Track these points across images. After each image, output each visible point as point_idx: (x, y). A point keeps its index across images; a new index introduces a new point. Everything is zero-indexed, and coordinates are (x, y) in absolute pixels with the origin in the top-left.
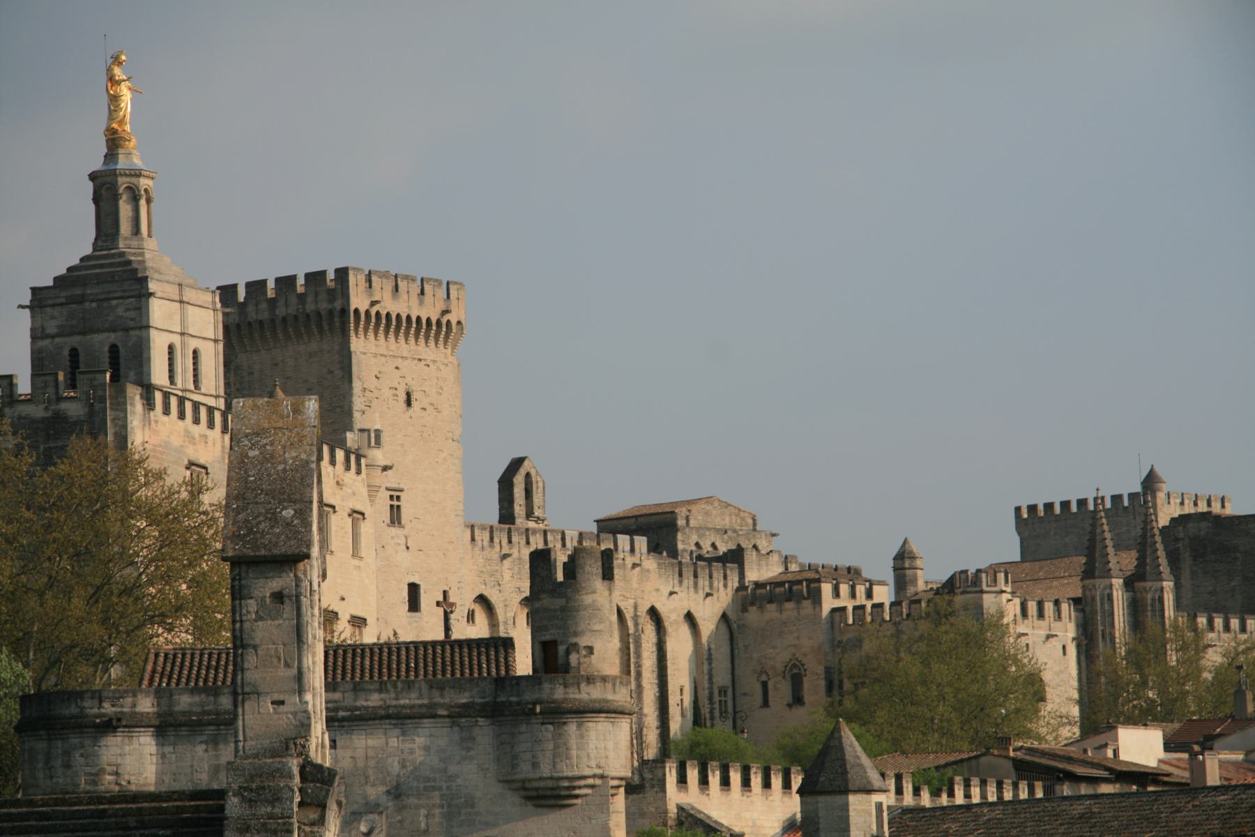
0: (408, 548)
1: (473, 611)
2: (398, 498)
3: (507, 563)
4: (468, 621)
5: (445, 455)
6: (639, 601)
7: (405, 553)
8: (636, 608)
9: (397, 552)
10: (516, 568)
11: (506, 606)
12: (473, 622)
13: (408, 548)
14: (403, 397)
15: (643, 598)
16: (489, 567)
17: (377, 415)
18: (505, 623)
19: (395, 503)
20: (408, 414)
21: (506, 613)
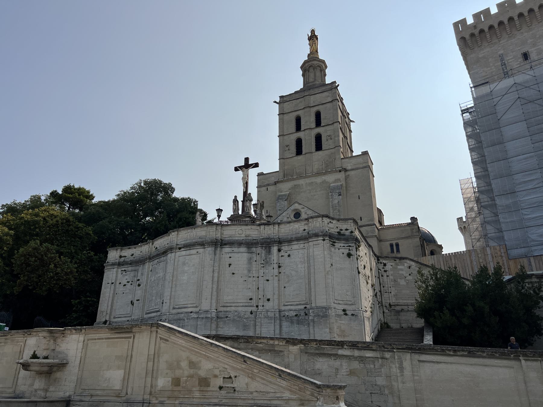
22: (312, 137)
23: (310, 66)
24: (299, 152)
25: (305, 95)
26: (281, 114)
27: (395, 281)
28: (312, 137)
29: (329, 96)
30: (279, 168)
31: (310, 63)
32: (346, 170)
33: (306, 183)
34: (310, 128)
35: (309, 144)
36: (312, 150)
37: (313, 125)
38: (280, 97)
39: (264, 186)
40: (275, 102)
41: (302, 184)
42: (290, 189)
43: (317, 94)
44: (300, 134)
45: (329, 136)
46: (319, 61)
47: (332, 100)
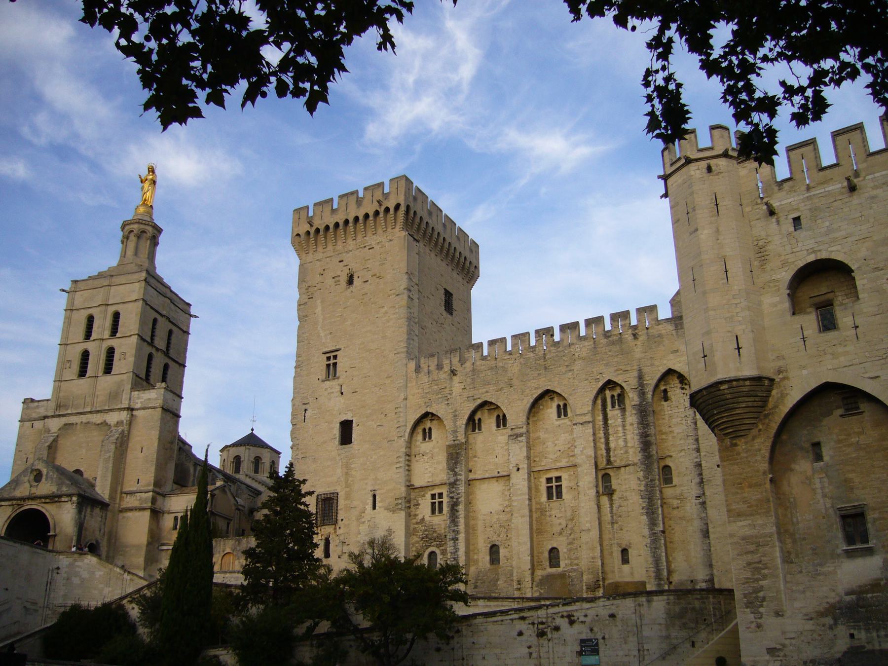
0: (342, 393)
1: (430, 429)
2: (335, 357)
3: (456, 379)
4: (424, 439)
5: (386, 308)
6: (646, 370)
7: (342, 399)
8: (640, 377)
9: (330, 399)
10: (469, 380)
11: (455, 416)
12: (430, 438)
13: (342, 393)
14: (344, 279)
15: (652, 365)
16: (436, 387)
17: (319, 302)
18: (455, 431)
19: (332, 361)
20: (349, 290)
21: (455, 422)
22: (103, 352)
23: (132, 231)
24: (82, 373)
25: (105, 284)
26: (70, 310)
27: (68, 579)
28: (103, 352)
29: (134, 291)
30: (52, 395)
31: (132, 226)
32: (131, 409)
33: (82, 422)
34: (101, 339)
35: (96, 363)
36: (99, 373)
37: (107, 334)
38: (72, 281)
39: (29, 421)
40: (63, 290)
41: (77, 424)
42: (60, 429)
43: (120, 286)
44: (90, 346)
45: (124, 354)
46: (145, 224)
47: (136, 300)
